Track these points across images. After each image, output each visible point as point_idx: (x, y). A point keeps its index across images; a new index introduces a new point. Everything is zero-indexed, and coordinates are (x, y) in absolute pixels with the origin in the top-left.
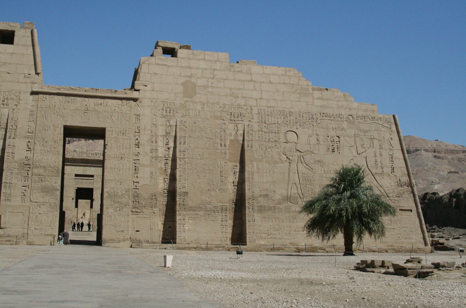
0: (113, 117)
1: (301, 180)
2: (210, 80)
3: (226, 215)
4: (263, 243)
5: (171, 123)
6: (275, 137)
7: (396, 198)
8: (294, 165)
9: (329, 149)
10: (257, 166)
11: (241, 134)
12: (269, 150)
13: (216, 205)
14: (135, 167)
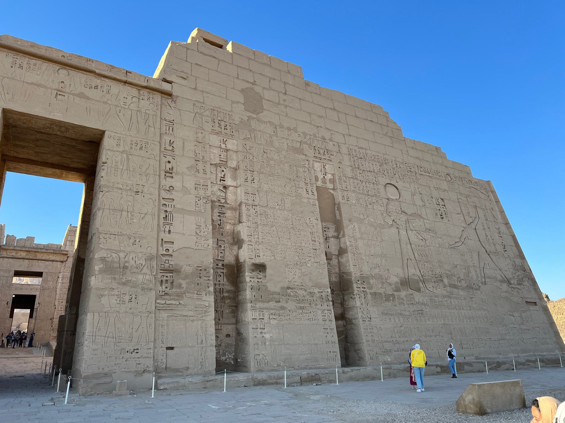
0: (121, 115)
1: (416, 255)
2: (281, 95)
3: (329, 308)
4: (389, 360)
5: (229, 147)
6: (374, 189)
7: (517, 286)
8: (403, 233)
9: (436, 214)
10: (359, 228)
11: (330, 180)
12: (370, 206)
13: (311, 290)
14: (166, 211)
